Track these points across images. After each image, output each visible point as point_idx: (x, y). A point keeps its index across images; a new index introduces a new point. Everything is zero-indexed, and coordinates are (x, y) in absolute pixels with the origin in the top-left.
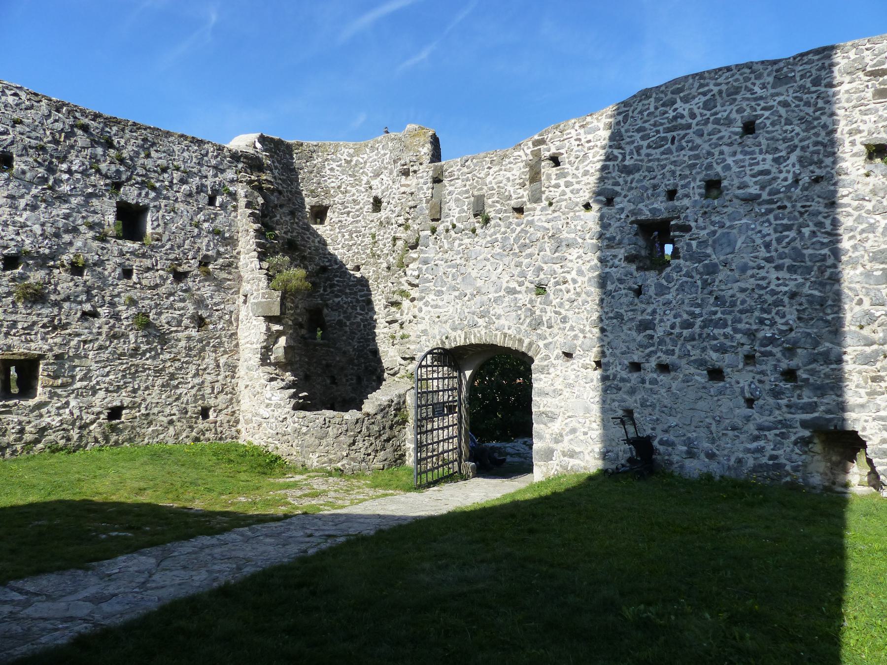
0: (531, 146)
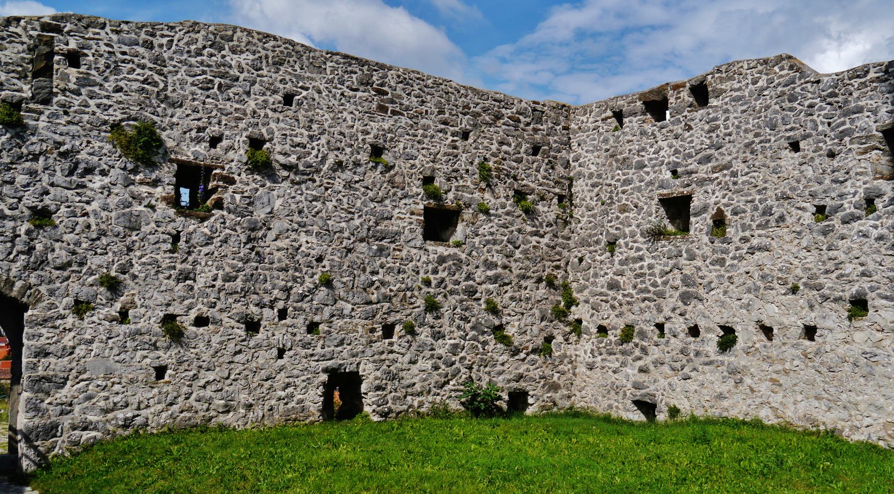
0: (39, 29)
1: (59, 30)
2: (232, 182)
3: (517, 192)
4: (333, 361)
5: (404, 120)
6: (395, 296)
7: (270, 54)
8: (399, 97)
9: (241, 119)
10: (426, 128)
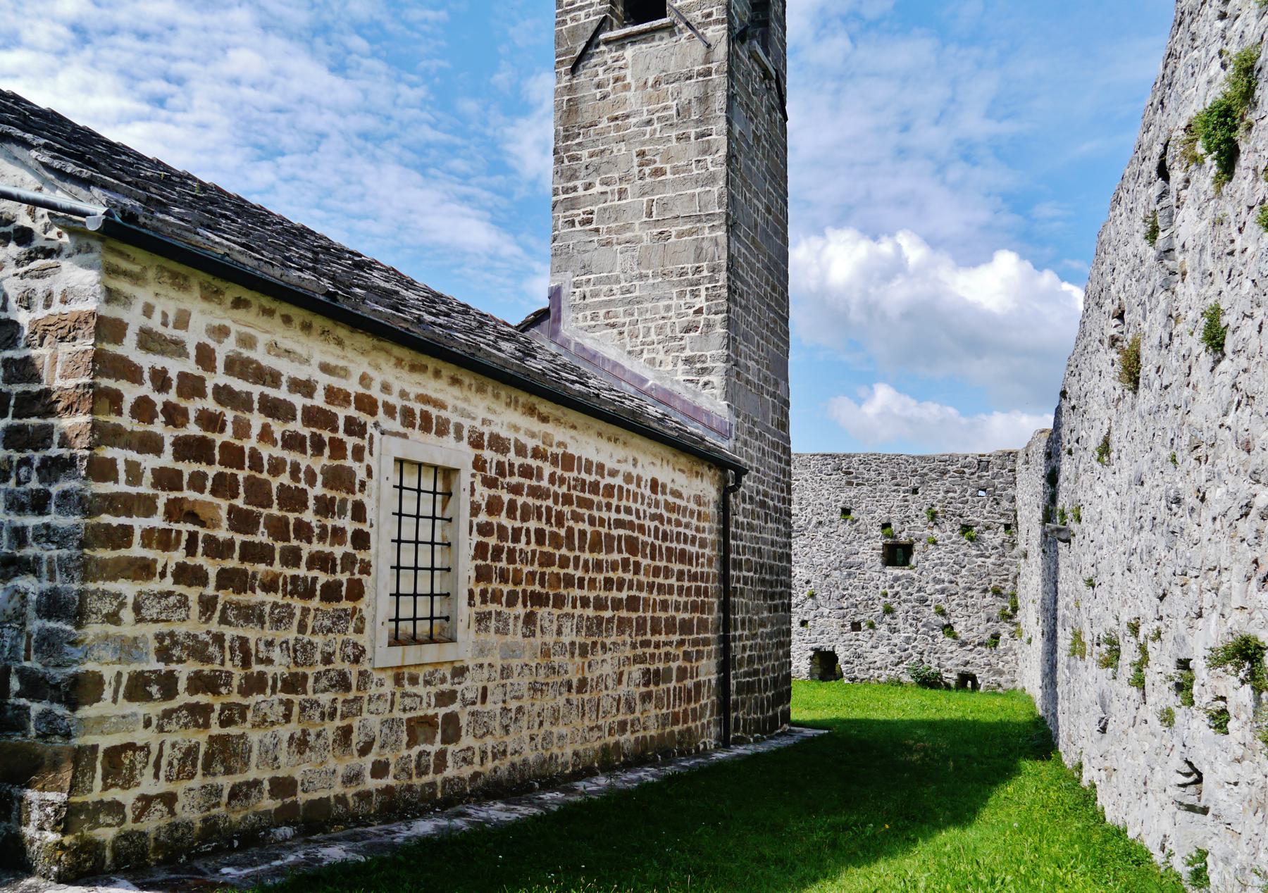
3: (963, 526)
5: (865, 488)
8: (862, 473)
10: (882, 491)
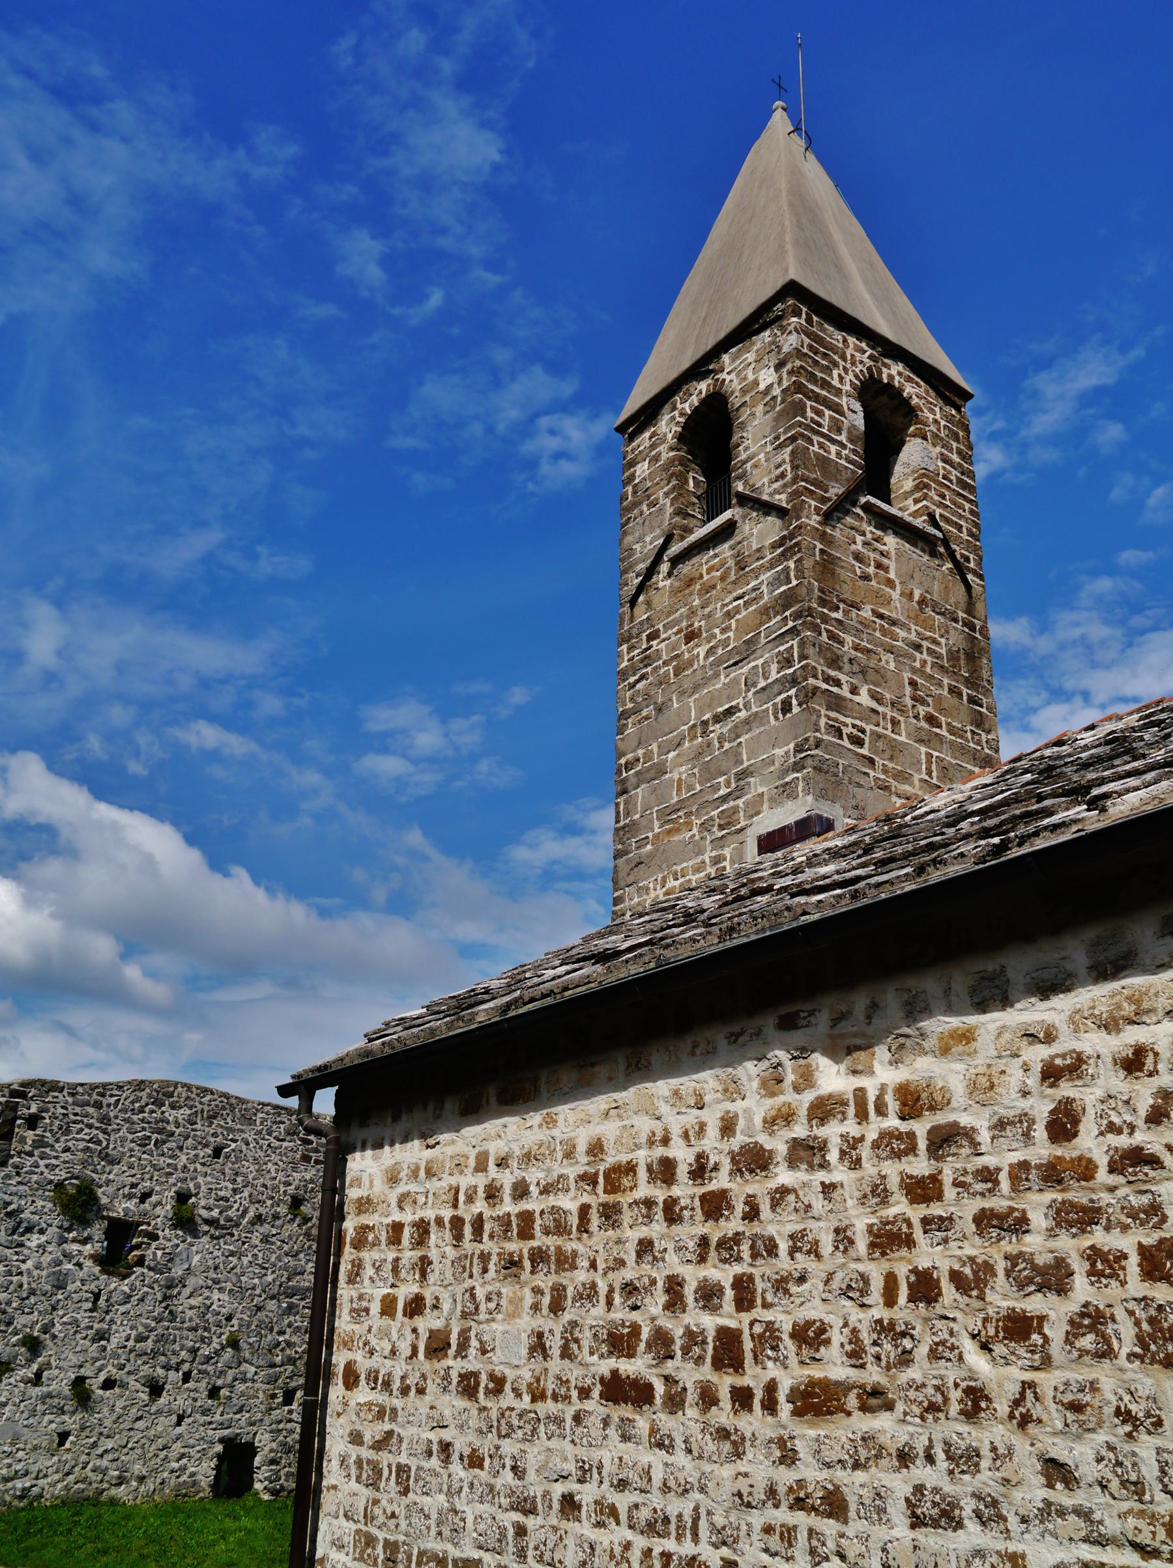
1: (23, 1095)
2: (154, 1237)
4: (230, 1430)
6: (300, 1358)
7: (206, 1108)
9: (172, 1174)
